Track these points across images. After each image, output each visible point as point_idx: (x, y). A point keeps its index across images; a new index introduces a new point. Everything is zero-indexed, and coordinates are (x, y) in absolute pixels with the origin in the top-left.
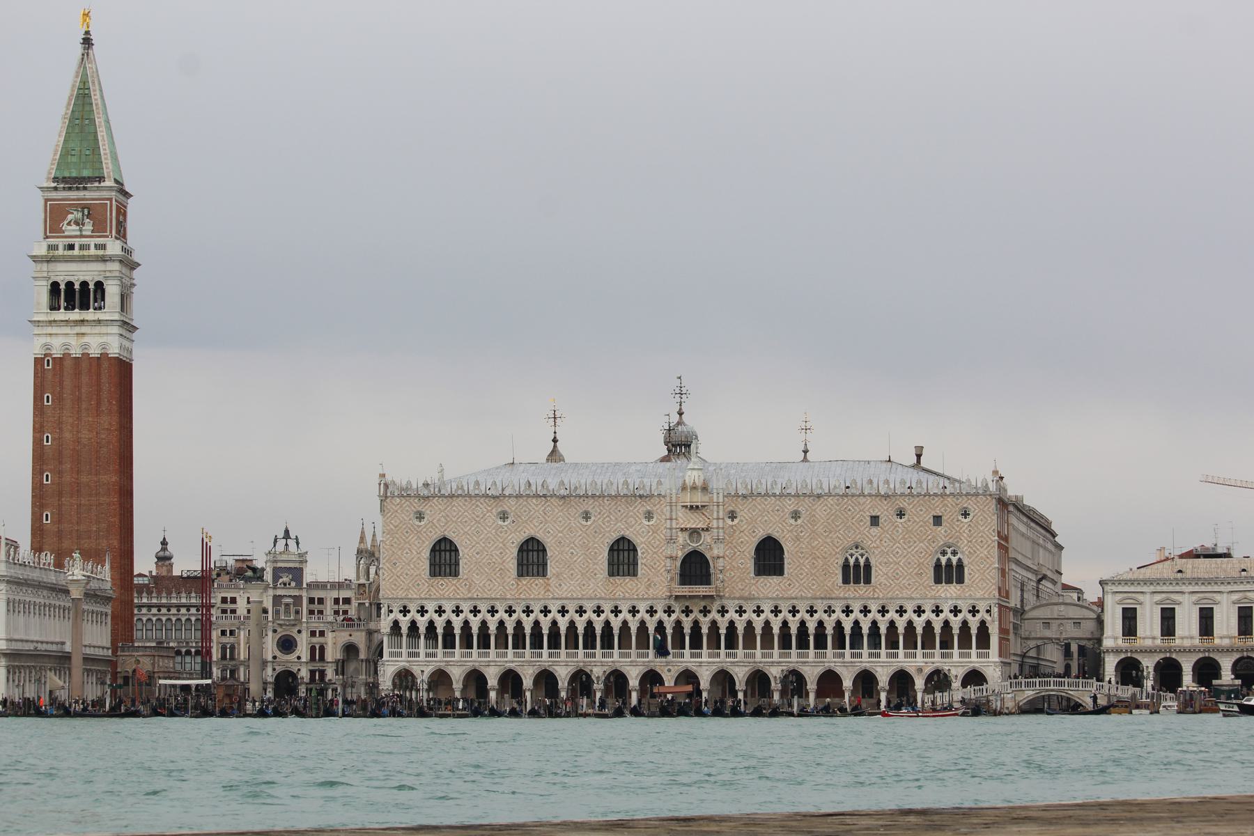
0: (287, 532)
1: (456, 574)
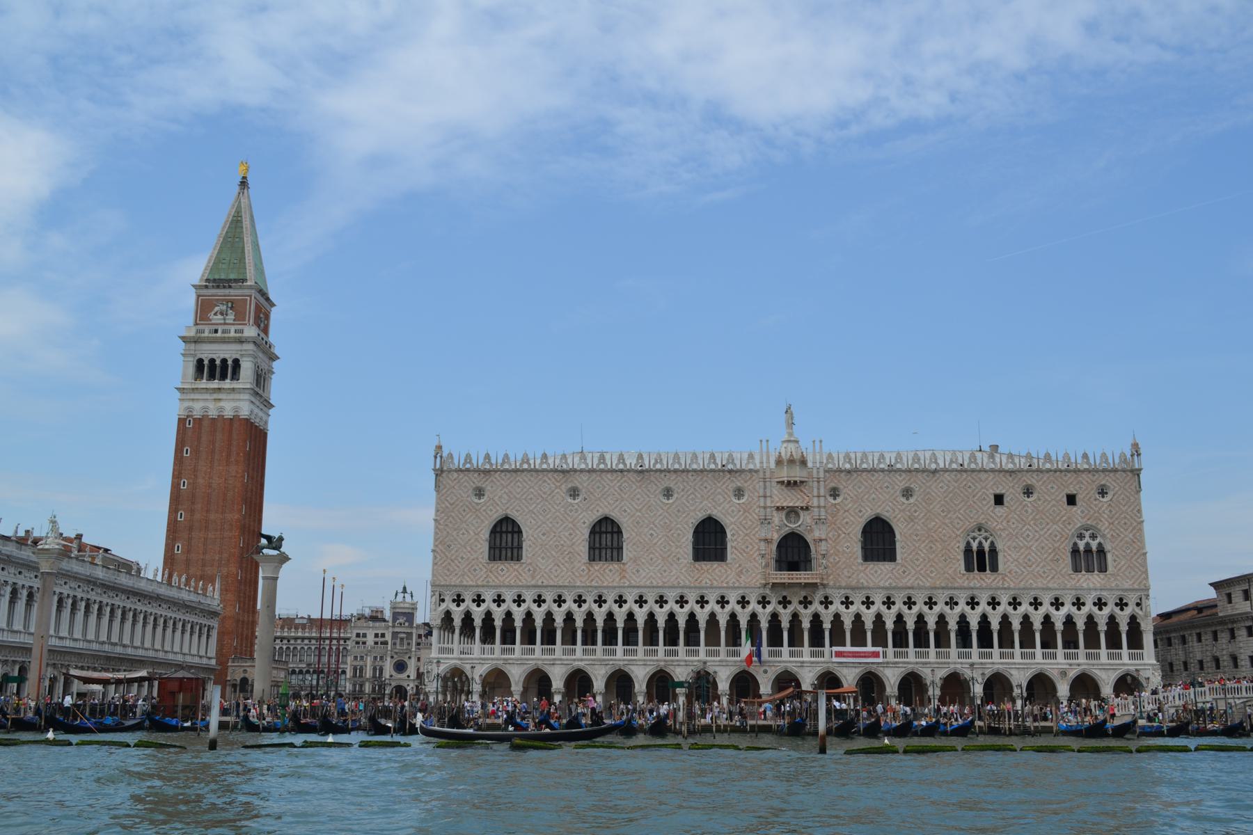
0: (405, 588)
1: (519, 558)
